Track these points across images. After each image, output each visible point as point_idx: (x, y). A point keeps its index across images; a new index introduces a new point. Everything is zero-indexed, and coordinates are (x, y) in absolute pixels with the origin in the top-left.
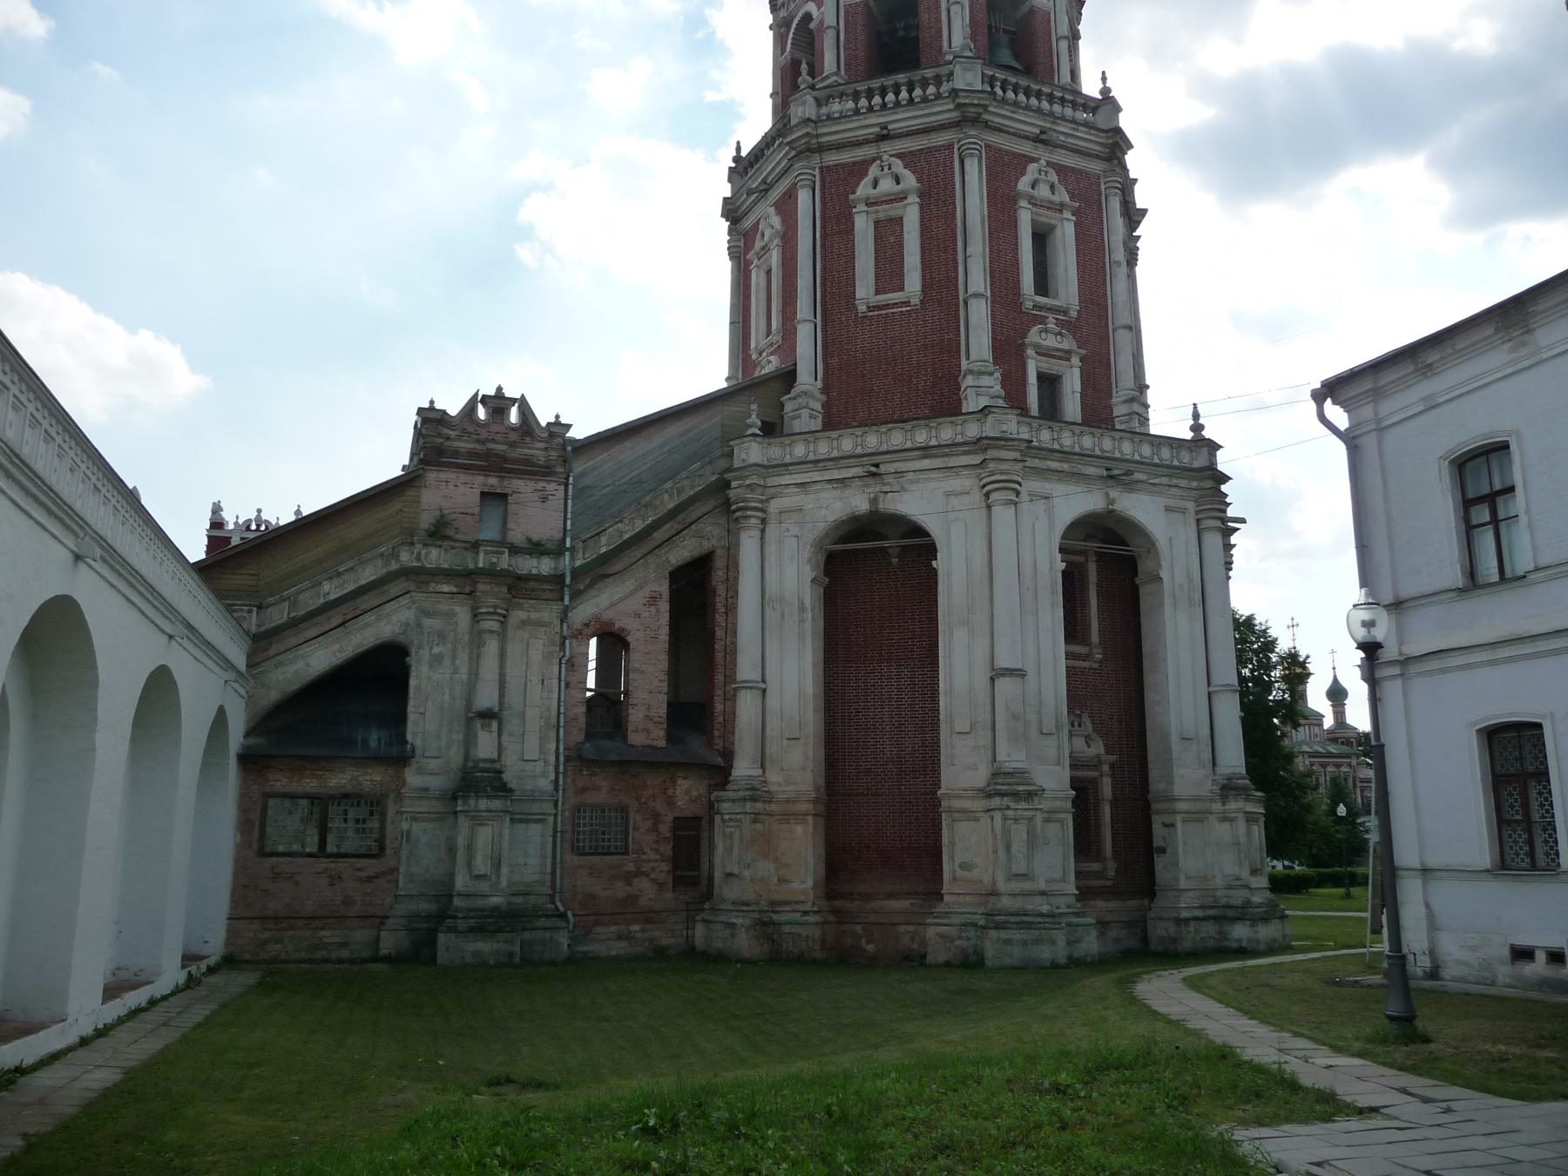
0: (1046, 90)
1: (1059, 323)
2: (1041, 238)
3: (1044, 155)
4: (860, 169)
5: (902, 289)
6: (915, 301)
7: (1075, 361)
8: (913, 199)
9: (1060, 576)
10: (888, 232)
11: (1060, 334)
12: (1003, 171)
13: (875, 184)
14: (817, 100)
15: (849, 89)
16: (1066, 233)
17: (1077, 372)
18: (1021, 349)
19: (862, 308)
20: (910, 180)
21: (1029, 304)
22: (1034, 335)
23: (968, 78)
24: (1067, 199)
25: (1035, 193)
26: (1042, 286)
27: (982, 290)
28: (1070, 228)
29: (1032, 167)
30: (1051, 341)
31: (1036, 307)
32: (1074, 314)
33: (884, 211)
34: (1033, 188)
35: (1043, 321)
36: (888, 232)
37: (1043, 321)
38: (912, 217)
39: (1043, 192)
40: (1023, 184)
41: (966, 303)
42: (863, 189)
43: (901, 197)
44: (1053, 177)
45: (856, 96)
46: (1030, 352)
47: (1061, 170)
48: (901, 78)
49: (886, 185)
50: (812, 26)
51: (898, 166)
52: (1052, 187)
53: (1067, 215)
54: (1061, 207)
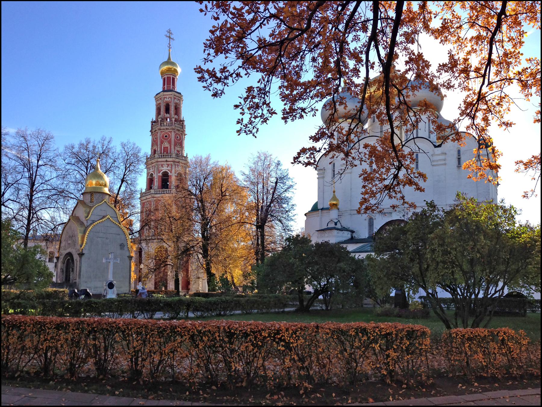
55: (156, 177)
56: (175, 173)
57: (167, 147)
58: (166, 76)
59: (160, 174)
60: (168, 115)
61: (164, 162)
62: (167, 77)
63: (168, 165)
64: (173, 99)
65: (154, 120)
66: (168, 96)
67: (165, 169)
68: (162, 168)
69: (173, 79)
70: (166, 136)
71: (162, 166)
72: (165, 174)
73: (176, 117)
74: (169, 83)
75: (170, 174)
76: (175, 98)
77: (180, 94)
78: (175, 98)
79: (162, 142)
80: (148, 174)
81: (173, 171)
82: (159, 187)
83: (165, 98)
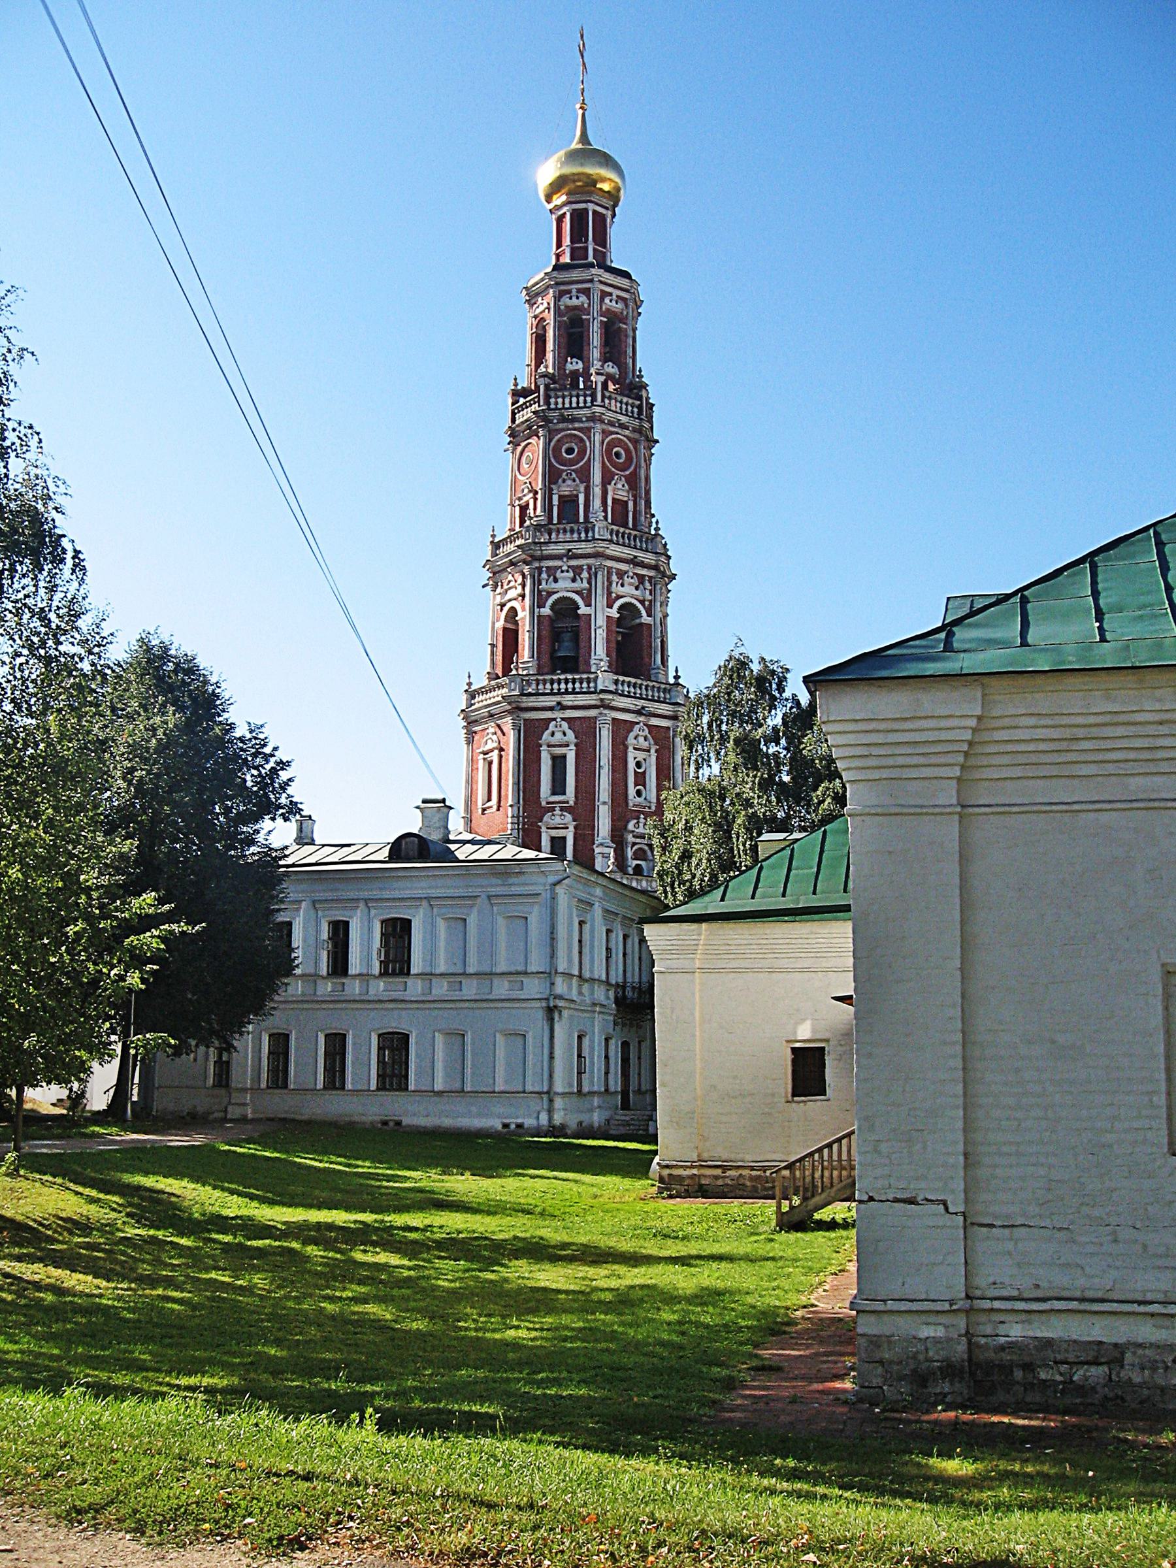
5: (564, 793)
8: (572, 747)
10: (559, 763)
12: (621, 730)
13: (553, 734)
19: (544, 804)
20: (571, 736)
21: (631, 804)
29: (637, 727)
33: (558, 751)
36: (559, 763)
40: (631, 740)
48: (570, 677)
51: (565, 725)
59: (546, 611)
60: (574, 365)
62: (574, 213)
63: (577, 571)
65: (523, 383)
66: (574, 287)
67: (564, 587)
68: (554, 585)
69: (600, 220)
70: (570, 451)
71: (551, 571)
72: (565, 608)
73: (611, 368)
74: (579, 232)
75: (583, 610)
76: (604, 294)
77: (626, 275)
82: (539, 667)
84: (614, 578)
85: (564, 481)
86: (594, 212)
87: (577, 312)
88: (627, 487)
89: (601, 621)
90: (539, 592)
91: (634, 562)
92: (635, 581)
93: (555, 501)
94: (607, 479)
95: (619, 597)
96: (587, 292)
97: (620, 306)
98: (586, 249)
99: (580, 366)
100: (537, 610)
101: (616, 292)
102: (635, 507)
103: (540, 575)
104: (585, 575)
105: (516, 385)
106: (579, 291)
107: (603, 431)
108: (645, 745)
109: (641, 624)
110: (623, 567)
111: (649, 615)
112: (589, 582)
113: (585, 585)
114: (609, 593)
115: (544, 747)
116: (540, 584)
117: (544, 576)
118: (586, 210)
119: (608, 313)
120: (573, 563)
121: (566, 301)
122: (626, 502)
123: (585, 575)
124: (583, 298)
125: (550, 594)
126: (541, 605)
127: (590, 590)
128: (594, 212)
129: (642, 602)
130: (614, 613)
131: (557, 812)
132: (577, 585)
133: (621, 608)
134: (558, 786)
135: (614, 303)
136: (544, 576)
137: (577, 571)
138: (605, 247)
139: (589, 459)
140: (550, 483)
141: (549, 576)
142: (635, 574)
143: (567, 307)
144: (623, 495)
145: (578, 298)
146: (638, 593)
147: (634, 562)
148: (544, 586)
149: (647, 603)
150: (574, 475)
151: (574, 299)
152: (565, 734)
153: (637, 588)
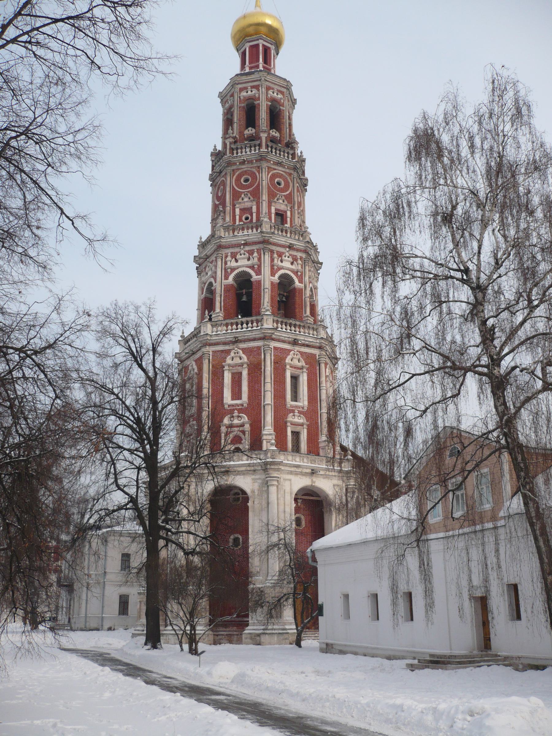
0: (298, 323)
1: (299, 412)
2: (295, 378)
3: (297, 348)
4: (228, 352)
6: (245, 405)
7: (305, 426)
9: (294, 509)
11: (299, 416)
13: (233, 359)
14: (212, 325)
15: (224, 322)
16: (304, 379)
17: (305, 431)
18: (286, 423)
19: (226, 406)
20: (245, 359)
21: (288, 406)
22: (290, 418)
23: (268, 323)
24: (304, 364)
25: (292, 363)
26: (295, 397)
27: (270, 403)
28: (305, 378)
29: (292, 352)
30: (296, 420)
31: (292, 406)
32: (306, 408)
34: (292, 360)
35: (293, 411)
37: (293, 411)
38: (245, 373)
39: (296, 362)
40: (288, 360)
41: (264, 406)
42: (229, 361)
43: (241, 365)
44: (299, 356)
45: (227, 325)
46: (289, 424)
47: (302, 353)
49: (237, 361)
50: (213, 288)
52: (299, 361)
53: (305, 370)
54: (302, 368)
55: (218, 291)
56: (273, 274)
57: (249, 210)
58: (247, 46)
60: (250, 131)
61: (238, 245)
64: (264, 90)
65: (219, 148)
69: (266, 50)
70: (246, 180)
71: (234, 256)
73: (274, 133)
74: (254, 58)
75: (255, 277)
76: (268, 88)
78: (268, 88)
79: (236, 196)
80: (202, 283)
81: (266, 269)
83: (241, 90)
84: (275, 255)
85: (243, 199)
86: (263, 45)
87: (251, 100)
88: (286, 202)
89: (267, 285)
90: (225, 270)
91: (291, 247)
92: (290, 259)
93: (237, 211)
94: (272, 196)
95: (280, 269)
96: (257, 87)
97: (280, 96)
98: (259, 65)
99: (254, 131)
100: (223, 281)
101: (276, 87)
102: (291, 214)
103: (226, 257)
104: (255, 254)
105: (215, 149)
106: (252, 87)
107: (269, 168)
108: (300, 364)
109: (295, 289)
110: (281, 250)
111: (301, 281)
112: (259, 259)
113: (256, 260)
114: (272, 266)
115: (226, 368)
116: (226, 263)
117: (229, 258)
118: (257, 46)
119: (273, 100)
120: (247, 248)
121: (244, 94)
122: (286, 212)
123: (255, 254)
124: (255, 91)
125: (233, 270)
126: (226, 278)
127: (260, 266)
128: (263, 45)
129: (296, 273)
130: (276, 279)
131: (236, 414)
132: (250, 263)
133: (281, 277)
134: (236, 395)
135: (275, 94)
136: (229, 258)
137: (251, 253)
138: (270, 65)
139: (259, 184)
140: (233, 200)
141: (232, 257)
142: (290, 255)
143: (244, 97)
144: (282, 207)
145: (252, 91)
146: (293, 267)
147: (291, 247)
148: (229, 263)
149: (299, 273)
150: (249, 195)
151: (249, 93)
152: (240, 358)
153: (292, 263)
